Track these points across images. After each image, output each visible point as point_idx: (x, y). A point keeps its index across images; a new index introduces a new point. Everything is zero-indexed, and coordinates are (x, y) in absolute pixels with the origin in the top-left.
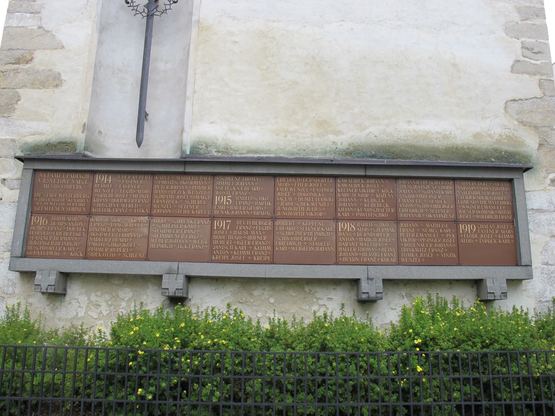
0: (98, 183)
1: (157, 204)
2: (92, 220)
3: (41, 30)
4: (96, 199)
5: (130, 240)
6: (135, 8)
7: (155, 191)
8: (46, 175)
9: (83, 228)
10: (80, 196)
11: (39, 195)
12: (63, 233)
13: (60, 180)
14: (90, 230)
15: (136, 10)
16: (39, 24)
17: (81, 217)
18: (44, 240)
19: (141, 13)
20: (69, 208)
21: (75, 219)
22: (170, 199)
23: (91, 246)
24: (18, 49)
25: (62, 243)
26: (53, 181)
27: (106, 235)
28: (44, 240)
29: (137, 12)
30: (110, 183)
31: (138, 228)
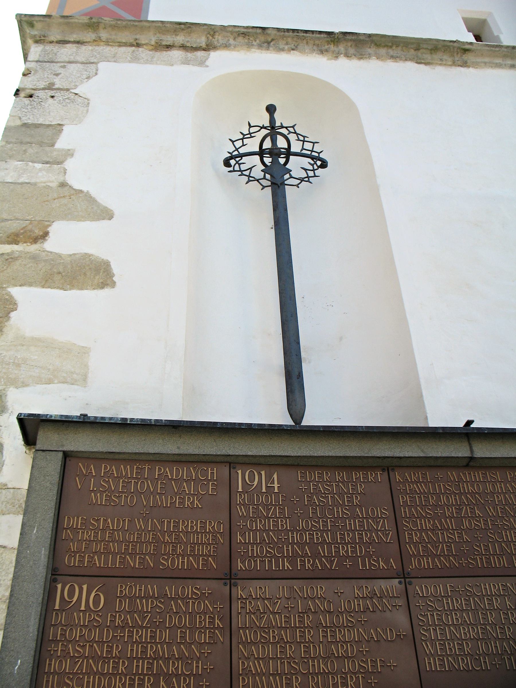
0: (244, 491)
1: (416, 544)
2: (239, 592)
3: (66, 188)
4: (243, 535)
5: (364, 648)
6: (247, 173)
7: (403, 512)
8: (98, 469)
9: (214, 618)
10: (196, 525)
11: (76, 522)
12: (155, 632)
13: (136, 483)
14: (238, 621)
15: (249, 176)
16: (61, 179)
17: (207, 587)
18: (96, 658)
19: (258, 180)
20: (167, 560)
21: (189, 591)
22: (447, 530)
23: (247, 672)
24: (17, 219)
25: (152, 664)
26: (117, 486)
27: (287, 636)
28: (96, 658)
29: (251, 179)
30: (276, 490)
31: (378, 612)
